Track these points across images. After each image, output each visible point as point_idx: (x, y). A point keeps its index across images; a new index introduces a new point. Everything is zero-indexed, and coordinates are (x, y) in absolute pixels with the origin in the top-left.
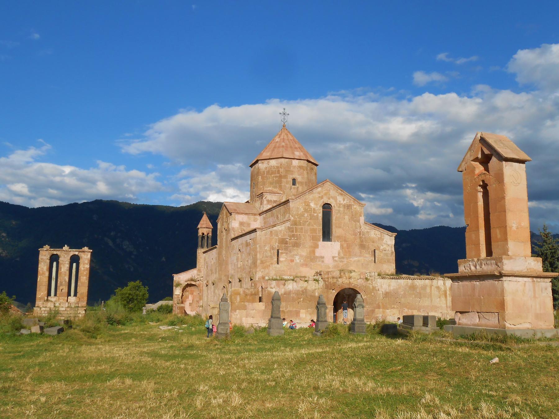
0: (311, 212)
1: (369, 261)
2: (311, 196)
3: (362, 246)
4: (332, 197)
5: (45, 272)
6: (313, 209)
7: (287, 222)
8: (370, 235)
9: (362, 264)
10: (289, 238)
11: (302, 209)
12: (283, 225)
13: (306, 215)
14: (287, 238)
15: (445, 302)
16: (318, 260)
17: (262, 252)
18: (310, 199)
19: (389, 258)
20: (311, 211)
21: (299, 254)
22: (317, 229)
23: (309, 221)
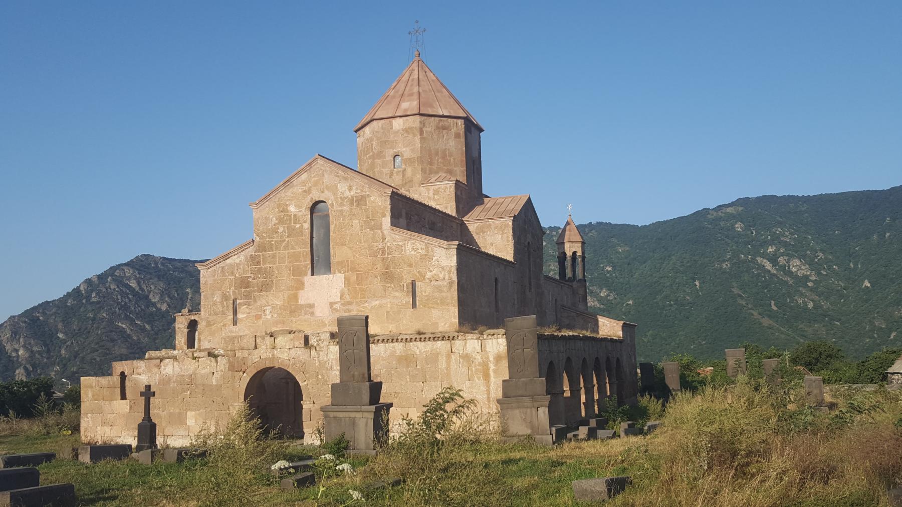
0: (291, 224)
1: (403, 305)
2: (289, 193)
3: (388, 277)
4: (327, 189)
5: (182, 346)
6: (292, 217)
7: (249, 247)
8: (403, 253)
9: (388, 312)
10: (252, 276)
11: (274, 219)
12: (241, 253)
13: (281, 230)
14: (250, 275)
15: (483, 388)
16: (303, 311)
17: (209, 306)
18: (288, 198)
19: (444, 294)
20: (290, 220)
21: (270, 304)
22: (300, 254)
23: (287, 240)
